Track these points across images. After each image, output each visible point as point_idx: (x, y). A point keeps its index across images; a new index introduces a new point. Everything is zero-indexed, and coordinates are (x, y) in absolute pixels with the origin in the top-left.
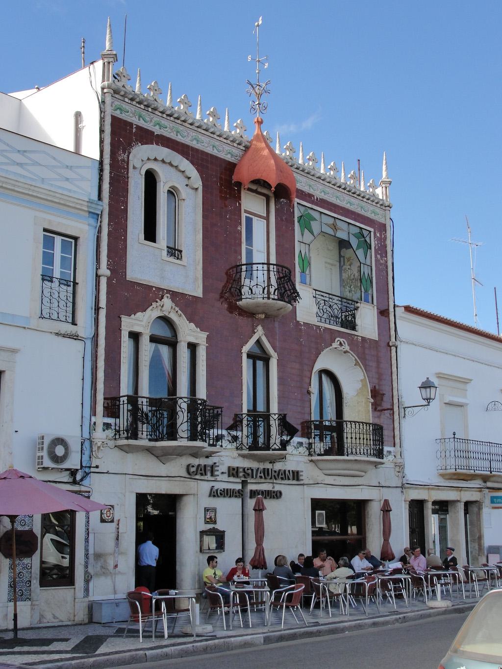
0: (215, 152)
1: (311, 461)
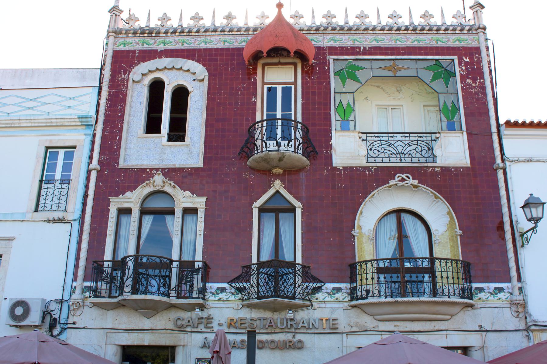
0: (227, 45)
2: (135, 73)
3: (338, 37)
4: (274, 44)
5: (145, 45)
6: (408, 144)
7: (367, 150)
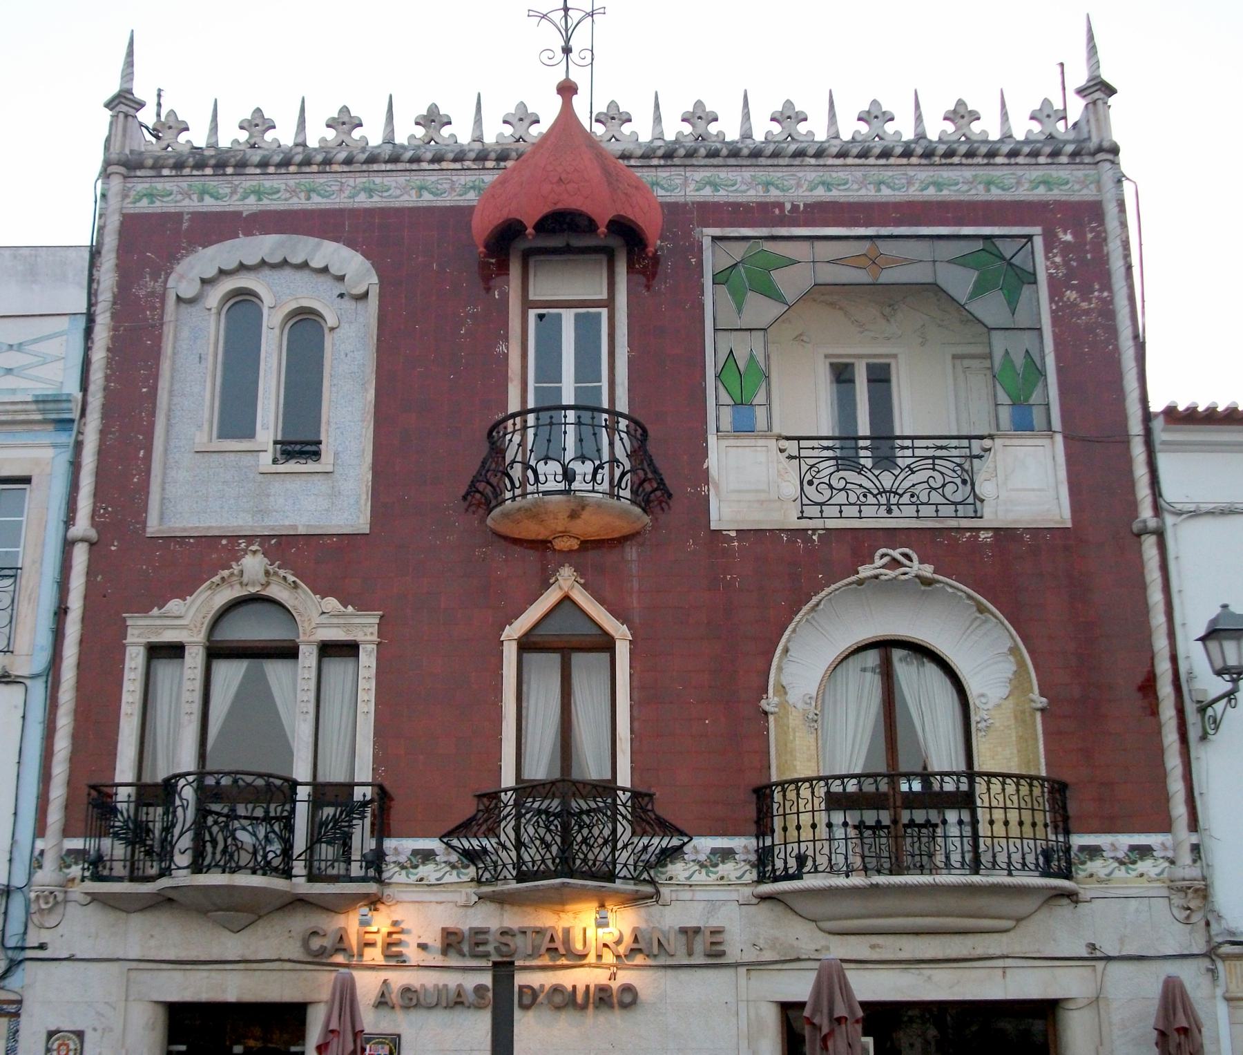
0: (427, 199)
1: (764, 898)
2: (182, 277)
3: (723, 174)
4: (555, 204)
5: (208, 200)
6: (908, 466)
7: (802, 483)
